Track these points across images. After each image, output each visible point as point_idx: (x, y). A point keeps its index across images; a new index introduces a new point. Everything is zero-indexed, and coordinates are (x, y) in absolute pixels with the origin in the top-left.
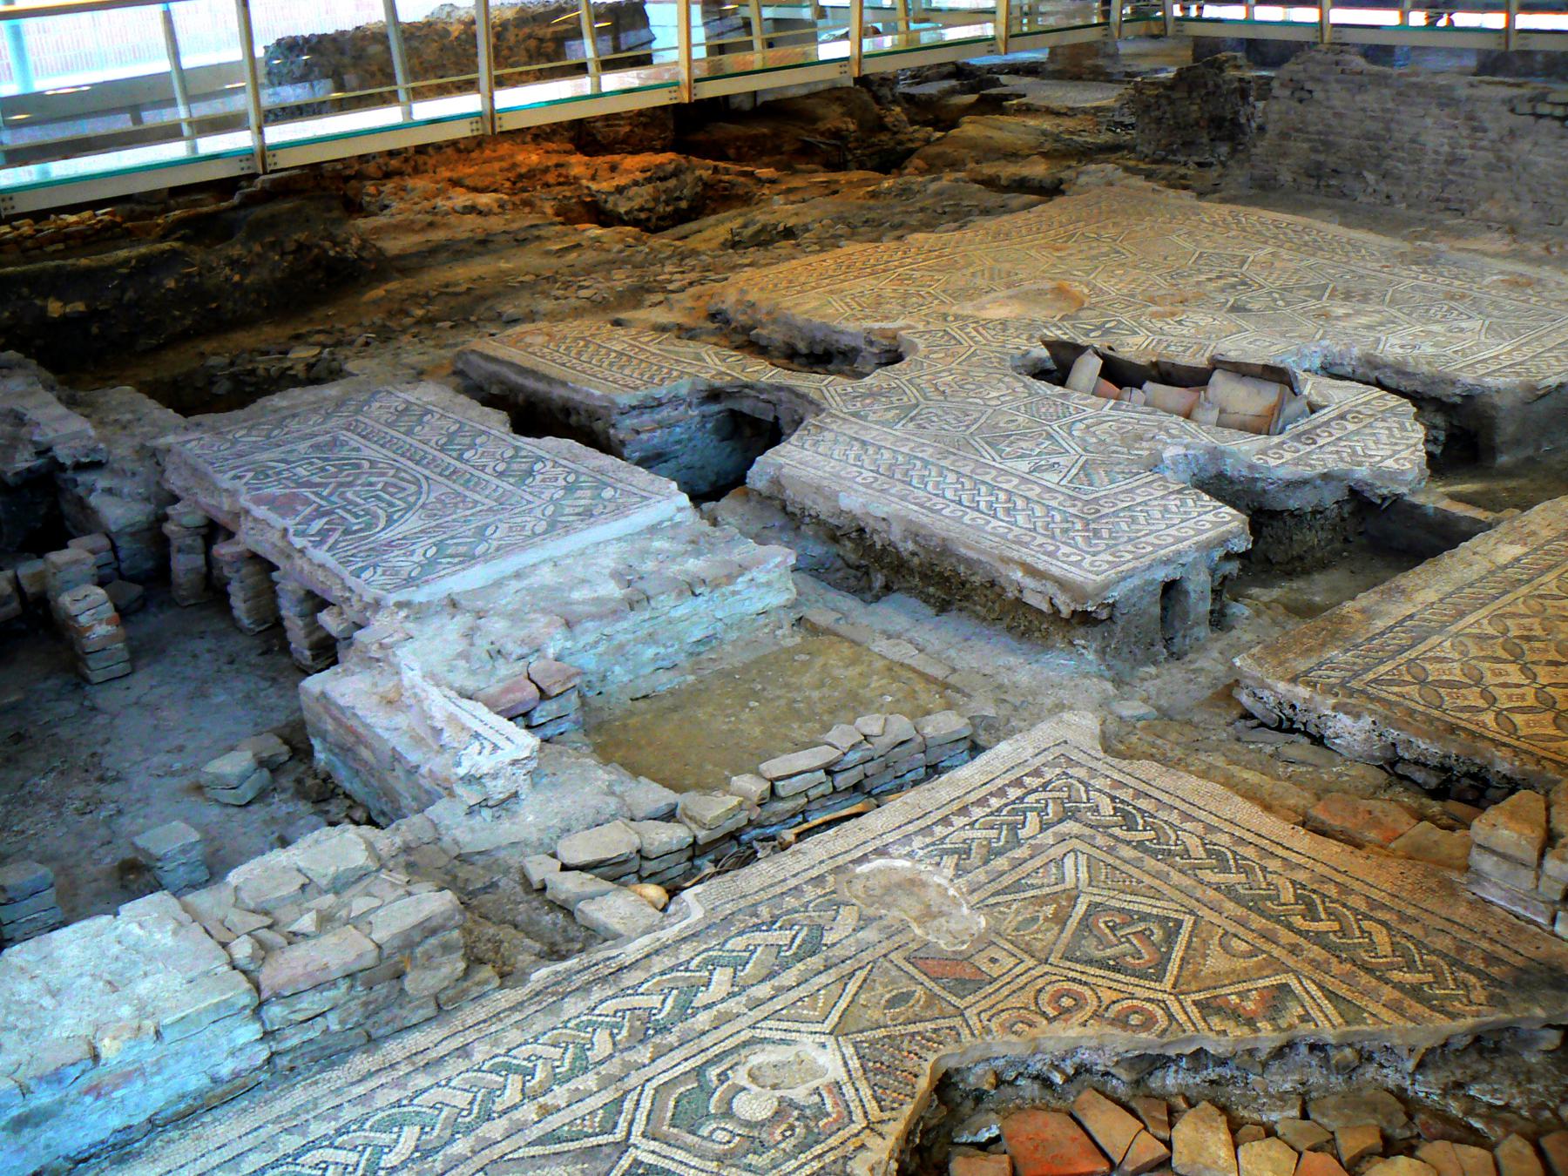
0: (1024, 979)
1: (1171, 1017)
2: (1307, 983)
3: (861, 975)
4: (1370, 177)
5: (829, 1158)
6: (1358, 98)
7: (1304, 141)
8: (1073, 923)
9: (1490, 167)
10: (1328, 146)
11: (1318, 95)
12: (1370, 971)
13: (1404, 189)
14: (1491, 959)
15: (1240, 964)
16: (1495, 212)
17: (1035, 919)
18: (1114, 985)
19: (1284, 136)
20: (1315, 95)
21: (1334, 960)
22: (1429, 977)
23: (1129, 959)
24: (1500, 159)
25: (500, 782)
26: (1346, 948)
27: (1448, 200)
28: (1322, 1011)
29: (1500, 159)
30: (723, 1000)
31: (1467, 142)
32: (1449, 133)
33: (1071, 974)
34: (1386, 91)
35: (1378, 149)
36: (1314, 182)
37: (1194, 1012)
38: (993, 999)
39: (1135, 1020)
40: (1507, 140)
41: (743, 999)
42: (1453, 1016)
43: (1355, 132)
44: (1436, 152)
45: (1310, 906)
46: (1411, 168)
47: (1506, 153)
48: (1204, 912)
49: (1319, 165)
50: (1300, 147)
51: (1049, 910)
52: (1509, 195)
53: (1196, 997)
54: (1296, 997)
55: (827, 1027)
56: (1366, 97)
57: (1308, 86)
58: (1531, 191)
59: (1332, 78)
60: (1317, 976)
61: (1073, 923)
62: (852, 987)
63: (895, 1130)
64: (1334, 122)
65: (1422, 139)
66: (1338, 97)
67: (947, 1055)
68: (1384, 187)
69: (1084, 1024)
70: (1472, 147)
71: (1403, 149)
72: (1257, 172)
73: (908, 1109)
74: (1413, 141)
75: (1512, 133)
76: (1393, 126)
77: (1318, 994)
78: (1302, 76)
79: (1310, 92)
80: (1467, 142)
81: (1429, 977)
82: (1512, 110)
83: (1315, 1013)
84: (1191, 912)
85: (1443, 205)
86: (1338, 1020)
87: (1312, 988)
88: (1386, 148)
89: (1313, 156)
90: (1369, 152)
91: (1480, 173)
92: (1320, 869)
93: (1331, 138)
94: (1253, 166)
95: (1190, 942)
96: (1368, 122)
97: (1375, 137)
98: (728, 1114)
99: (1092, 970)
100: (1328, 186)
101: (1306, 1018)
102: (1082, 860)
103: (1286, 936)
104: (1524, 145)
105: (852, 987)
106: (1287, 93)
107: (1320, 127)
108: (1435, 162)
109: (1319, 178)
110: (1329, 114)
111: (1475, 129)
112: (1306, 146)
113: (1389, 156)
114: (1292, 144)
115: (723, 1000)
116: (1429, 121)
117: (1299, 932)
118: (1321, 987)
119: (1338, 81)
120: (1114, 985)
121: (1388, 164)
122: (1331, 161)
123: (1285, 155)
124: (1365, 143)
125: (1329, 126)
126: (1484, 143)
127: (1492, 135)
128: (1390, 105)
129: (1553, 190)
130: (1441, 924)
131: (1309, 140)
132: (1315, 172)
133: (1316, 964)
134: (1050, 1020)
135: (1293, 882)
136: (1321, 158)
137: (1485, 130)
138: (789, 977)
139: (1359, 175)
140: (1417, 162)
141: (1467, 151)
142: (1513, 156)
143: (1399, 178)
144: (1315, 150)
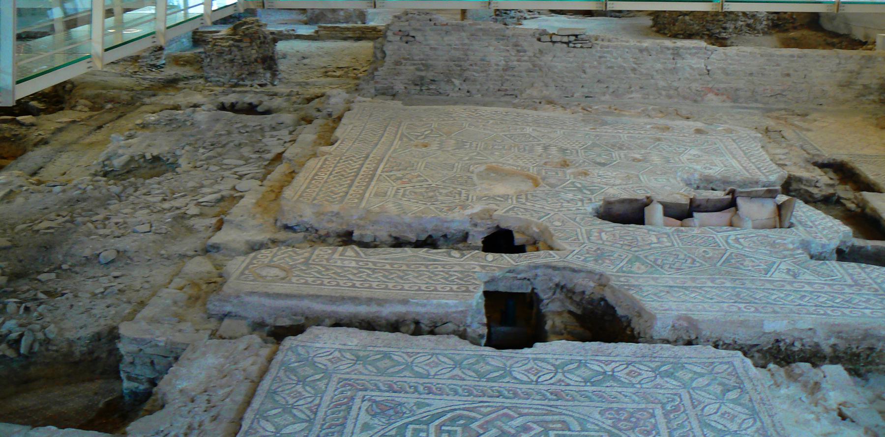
4: (457, 82)
6: (446, 38)
9: (529, 71)
10: (427, 67)
11: (419, 37)
13: (478, 87)
16: (535, 93)
19: (397, 63)
20: (417, 38)
24: (534, 66)
27: (506, 90)
29: (534, 66)
31: (515, 58)
32: (504, 54)
34: (463, 34)
35: (460, 66)
36: (418, 88)
40: (538, 55)
43: (444, 58)
44: (497, 65)
47: (538, 62)
50: (409, 70)
52: (542, 84)
57: (412, 34)
58: (554, 80)
59: (428, 28)
65: (487, 59)
66: (433, 39)
68: (465, 87)
70: (518, 61)
72: (379, 86)
74: (482, 60)
76: (469, 53)
78: (408, 28)
80: (515, 58)
82: (539, 40)
85: (503, 93)
88: (466, 65)
89: (419, 73)
90: (455, 68)
91: (524, 74)
93: (430, 62)
94: (376, 82)
96: (453, 52)
97: (459, 59)
100: (429, 89)
104: (548, 58)
106: (398, 38)
107: (422, 57)
108: (497, 70)
109: (422, 85)
110: (427, 49)
111: (518, 51)
112: (412, 68)
114: (402, 67)
116: (492, 49)
119: (432, 30)
122: (430, 75)
123: (398, 74)
124: (452, 64)
125: (427, 55)
126: (525, 58)
127: (530, 54)
128: (467, 41)
129: (566, 80)
131: (414, 64)
132: (419, 82)
136: (423, 74)
137: (525, 51)
139: (449, 81)
140: (486, 71)
141: (515, 63)
142: (542, 63)
143: (475, 81)
144: (419, 70)
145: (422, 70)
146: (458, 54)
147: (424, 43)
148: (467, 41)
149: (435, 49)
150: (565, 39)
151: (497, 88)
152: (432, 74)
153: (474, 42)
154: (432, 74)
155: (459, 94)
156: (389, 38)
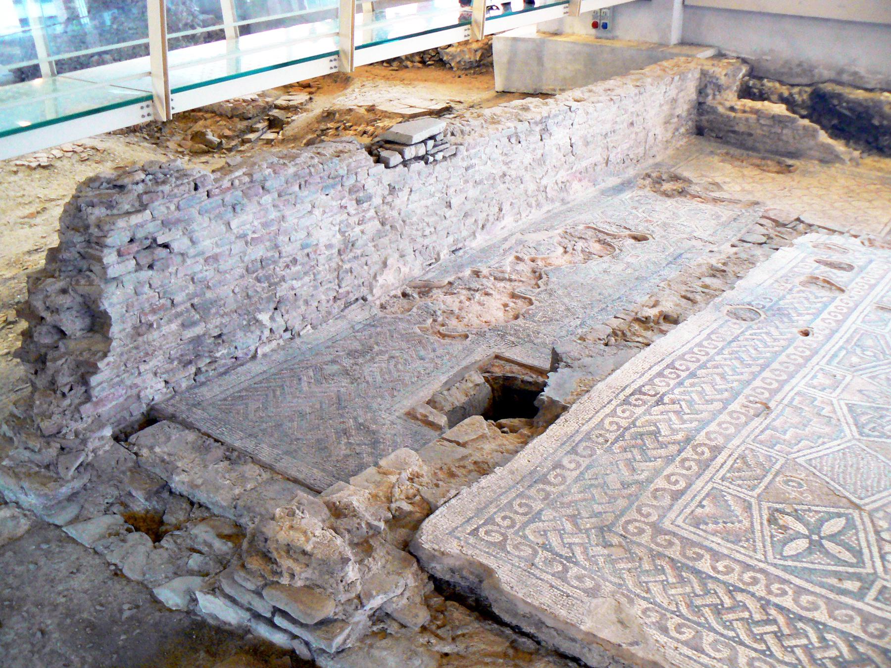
4: (264, 317)
7: (170, 321)
11: (179, 243)
20: (175, 246)
34: (267, 199)
46: (307, 279)
49: (197, 340)
56: (244, 217)
59: (194, 211)
64: (208, 273)
71: (295, 261)
75: (392, 189)
78: (151, 227)
79: (166, 246)
89: (189, 334)
93: (209, 295)
112: (174, 326)
113: (283, 279)
114: (155, 335)
121: (282, 291)
122: (213, 326)
124: (250, 280)
136: (198, 330)
145: (194, 324)
146: (258, 252)
147: (192, 252)
148: (273, 214)
149: (215, 258)
150: (422, 151)
151: (332, 294)
152: (218, 321)
153: (288, 212)
154: (218, 321)
155: (274, 344)
156: (111, 273)
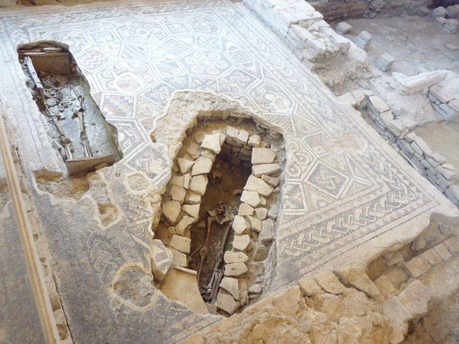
0: (311, 153)
1: (292, 177)
2: (304, 213)
3: (315, 124)
5: (252, 103)
8: (334, 170)
12: (306, 230)
14: (305, 265)
15: (314, 202)
17: (338, 163)
18: (307, 171)
21: (312, 224)
22: (300, 243)
23: (319, 178)
25: (394, 83)
26: (318, 230)
28: (290, 212)
30: (306, 100)
33: (313, 163)
37: (296, 183)
38: (303, 144)
39: (293, 170)
41: (306, 103)
42: (281, 241)
45: (341, 229)
48: (339, 202)
51: (343, 168)
53: (301, 187)
54: (297, 209)
55: (295, 113)
60: (305, 218)
61: (334, 170)
62: (310, 121)
63: (260, 115)
67: (285, 133)
69: (292, 159)
73: (265, 119)
77: (298, 214)
81: (300, 243)
83: (289, 210)
84: (339, 199)
86: (286, 214)
87: (301, 214)
92: (360, 241)
95: (325, 194)
98: (267, 93)
99: (314, 168)
101: (288, 207)
102: (370, 185)
103: (325, 217)
105: (310, 121)
115: (306, 100)
117: (327, 221)
118: (300, 216)
120: (307, 171)
130: (326, 258)
133: (311, 219)
134: (295, 153)
135: (354, 231)
138: (313, 111)
